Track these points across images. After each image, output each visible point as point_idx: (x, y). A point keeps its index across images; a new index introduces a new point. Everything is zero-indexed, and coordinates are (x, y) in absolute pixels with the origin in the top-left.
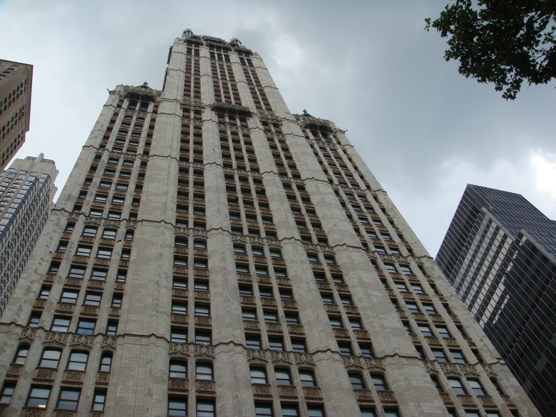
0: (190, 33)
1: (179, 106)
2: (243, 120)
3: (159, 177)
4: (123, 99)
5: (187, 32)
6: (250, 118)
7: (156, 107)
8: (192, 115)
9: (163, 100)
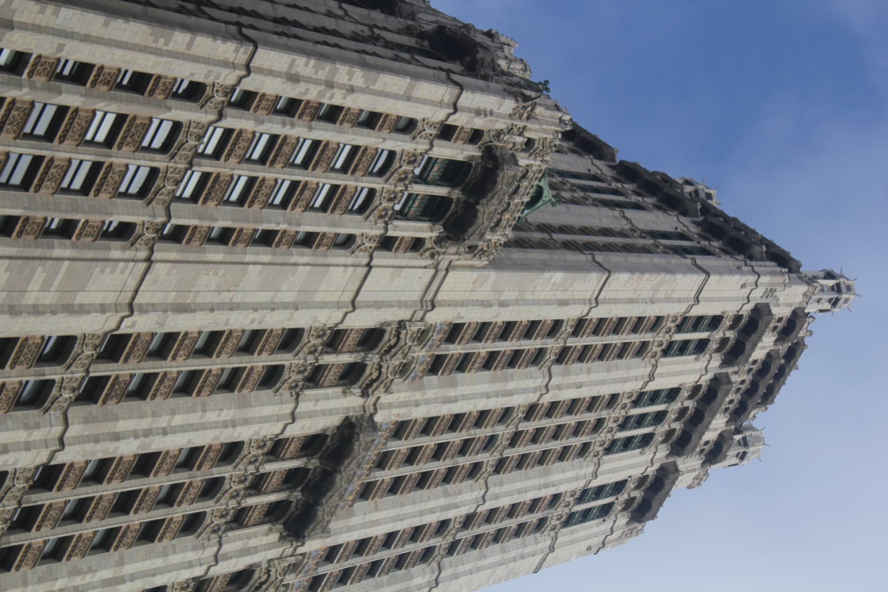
0: (827, 306)
1: (392, 315)
2: (273, 513)
3: (35, 284)
4: (485, 138)
5: (834, 296)
6: (274, 537)
7: (417, 245)
8: (346, 358)
9: (443, 265)
